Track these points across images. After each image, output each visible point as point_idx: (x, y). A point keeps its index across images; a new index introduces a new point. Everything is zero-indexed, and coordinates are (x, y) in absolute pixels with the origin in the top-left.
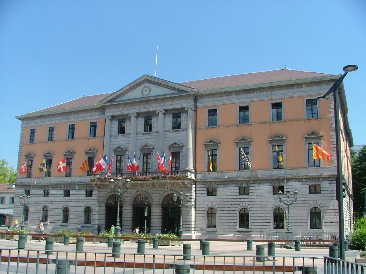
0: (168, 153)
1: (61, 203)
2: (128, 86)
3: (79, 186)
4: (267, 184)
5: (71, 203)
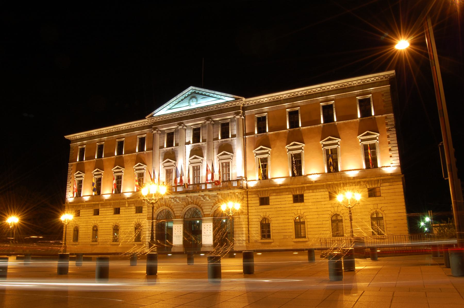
1: (111, 221)
4: (322, 190)
5: (121, 220)
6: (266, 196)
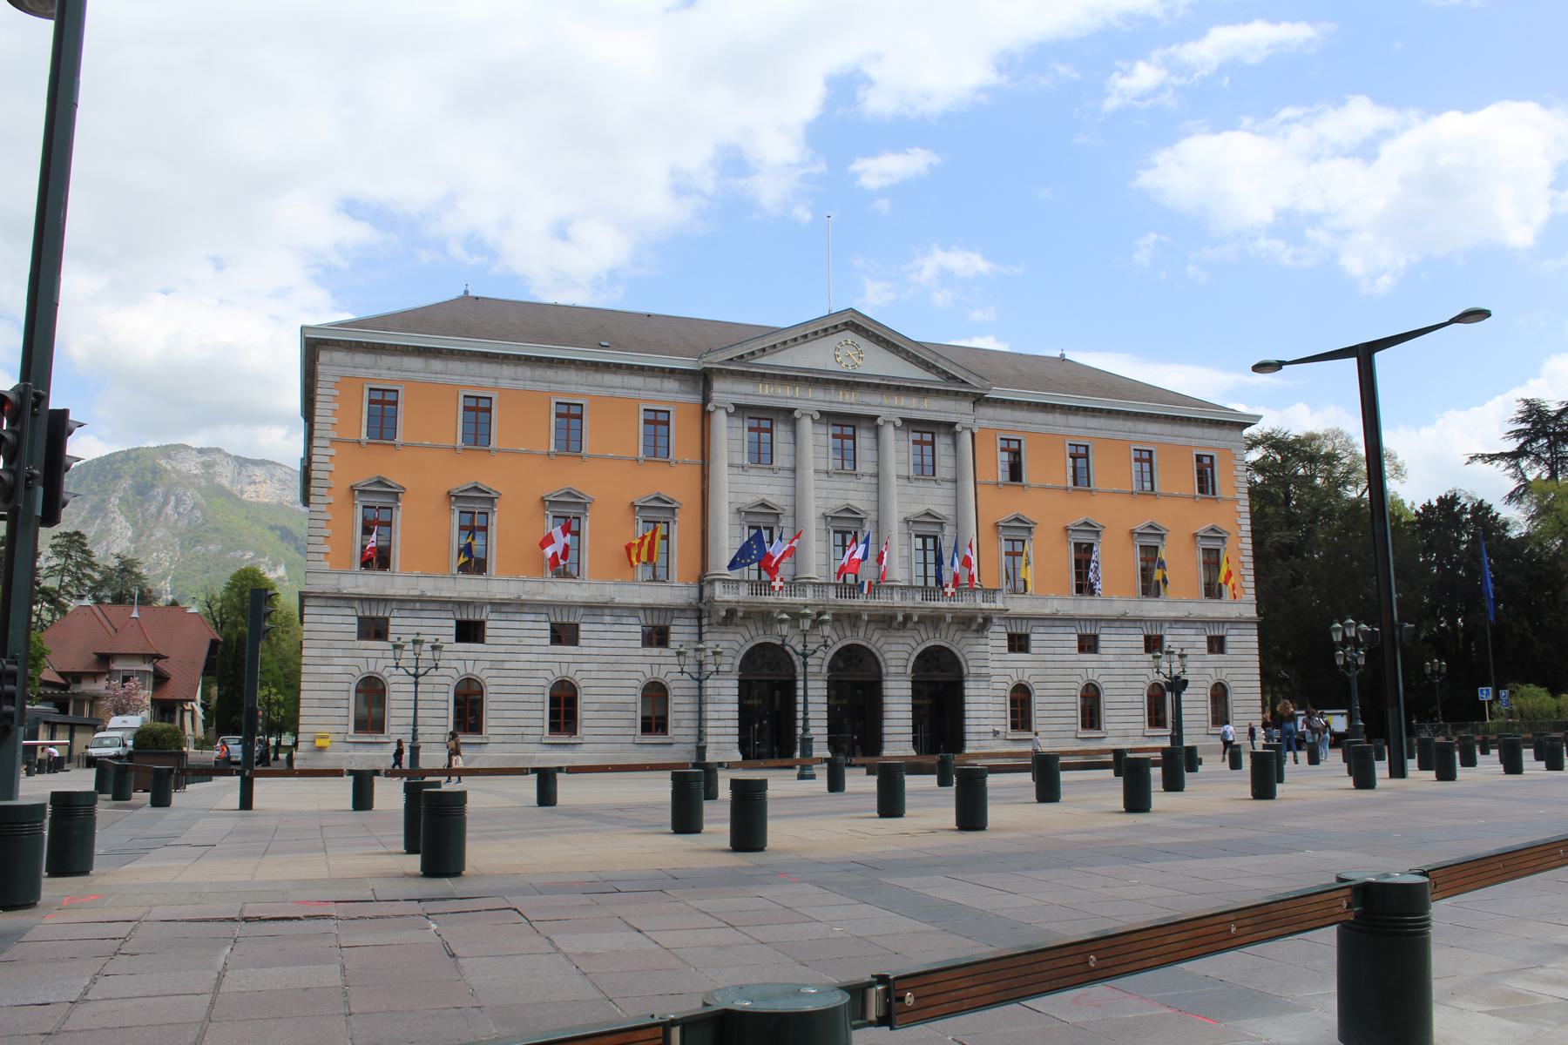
1: (542, 666)
3: (616, 612)
5: (585, 667)
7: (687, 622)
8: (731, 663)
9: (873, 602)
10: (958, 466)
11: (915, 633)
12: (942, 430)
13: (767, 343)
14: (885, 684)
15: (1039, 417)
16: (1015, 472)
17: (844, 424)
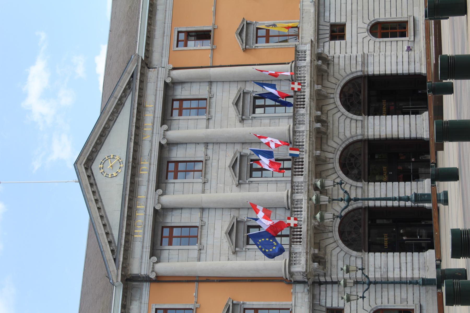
0: (254, 121)
2: (90, 203)
6: (328, 28)
7: (323, 293)
8: (355, 258)
9: (306, 147)
10: (199, 81)
11: (330, 114)
12: (170, 93)
13: (101, 231)
14: (371, 137)
15: (159, 16)
16: (204, 35)
17: (167, 170)
